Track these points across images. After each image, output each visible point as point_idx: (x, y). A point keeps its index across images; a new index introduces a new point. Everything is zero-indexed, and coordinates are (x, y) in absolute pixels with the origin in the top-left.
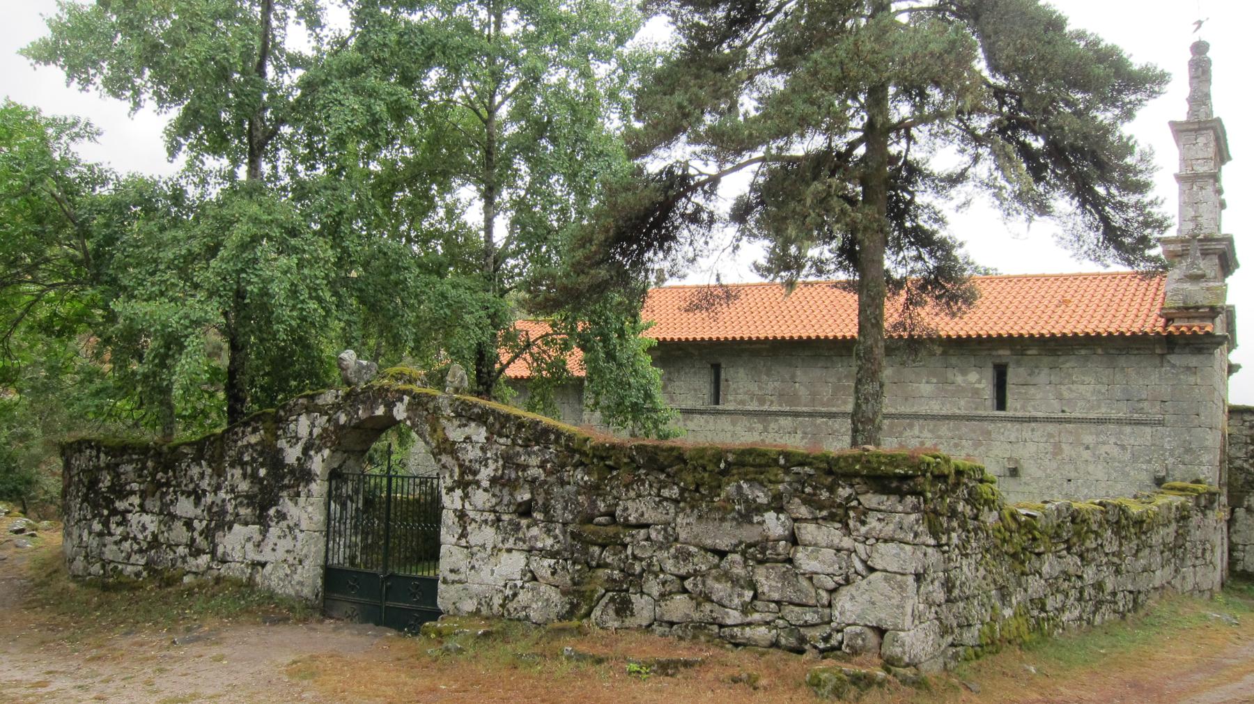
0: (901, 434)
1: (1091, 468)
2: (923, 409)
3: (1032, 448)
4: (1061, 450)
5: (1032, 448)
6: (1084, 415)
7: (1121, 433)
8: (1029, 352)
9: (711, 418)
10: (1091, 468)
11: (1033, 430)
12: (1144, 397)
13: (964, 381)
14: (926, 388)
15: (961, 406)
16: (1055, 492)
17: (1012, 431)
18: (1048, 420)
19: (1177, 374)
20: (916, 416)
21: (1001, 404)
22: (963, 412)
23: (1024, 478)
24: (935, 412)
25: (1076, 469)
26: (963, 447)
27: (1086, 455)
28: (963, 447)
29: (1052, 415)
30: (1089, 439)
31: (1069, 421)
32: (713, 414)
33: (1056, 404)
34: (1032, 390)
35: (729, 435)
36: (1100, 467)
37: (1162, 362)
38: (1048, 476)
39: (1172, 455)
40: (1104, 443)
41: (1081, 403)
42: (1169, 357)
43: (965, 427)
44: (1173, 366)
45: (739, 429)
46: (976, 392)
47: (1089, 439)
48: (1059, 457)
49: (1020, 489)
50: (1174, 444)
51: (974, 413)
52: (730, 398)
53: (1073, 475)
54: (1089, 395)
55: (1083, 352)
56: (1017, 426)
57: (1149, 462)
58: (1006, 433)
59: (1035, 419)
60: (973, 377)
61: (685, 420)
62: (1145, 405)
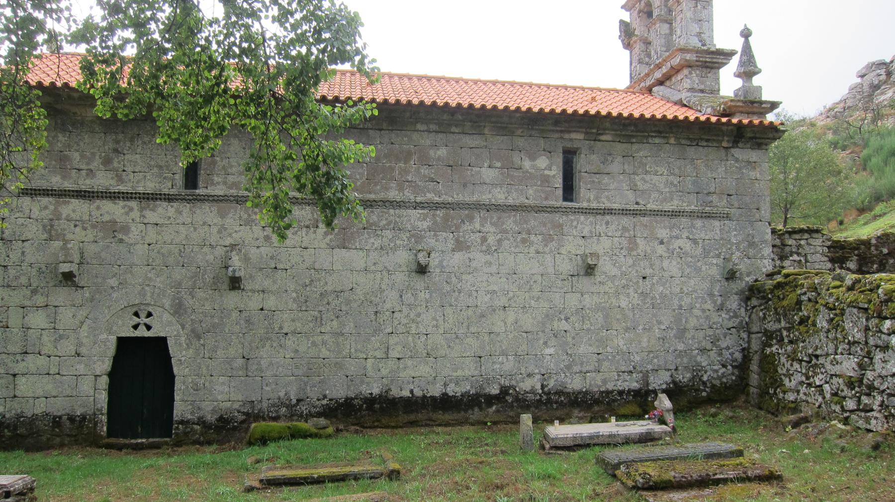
0: (458, 228)
1: (665, 264)
2: (486, 198)
3: (606, 243)
4: (636, 245)
5: (606, 243)
6: (660, 208)
7: (693, 226)
8: (603, 138)
9: (186, 208)
10: (665, 264)
11: (607, 223)
12: (712, 190)
13: (533, 167)
14: (488, 174)
15: (531, 195)
16: (631, 291)
17: (585, 224)
18: (624, 212)
19: (740, 169)
20: (478, 206)
21: (569, 191)
22: (531, 202)
23: (599, 277)
24: (500, 202)
25: (651, 265)
26: (532, 243)
27: (661, 250)
28: (532, 243)
29: (628, 207)
30: (663, 233)
31: (643, 213)
32: (189, 201)
33: (631, 195)
34: (606, 179)
35: (215, 230)
36: (674, 263)
37: (727, 155)
38: (623, 274)
39: (738, 249)
40: (677, 238)
41: (655, 195)
42: (733, 150)
43: (534, 220)
44: (737, 160)
45: (229, 221)
46: (546, 180)
47: (663, 233)
48: (635, 253)
49: (594, 289)
50: (740, 238)
51: (545, 203)
52: (216, 179)
53: (648, 271)
54: (662, 186)
55: (657, 140)
56: (591, 218)
57: (718, 256)
58: (580, 226)
59: (610, 211)
60: (542, 162)
61: (142, 209)
62: (714, 198)
